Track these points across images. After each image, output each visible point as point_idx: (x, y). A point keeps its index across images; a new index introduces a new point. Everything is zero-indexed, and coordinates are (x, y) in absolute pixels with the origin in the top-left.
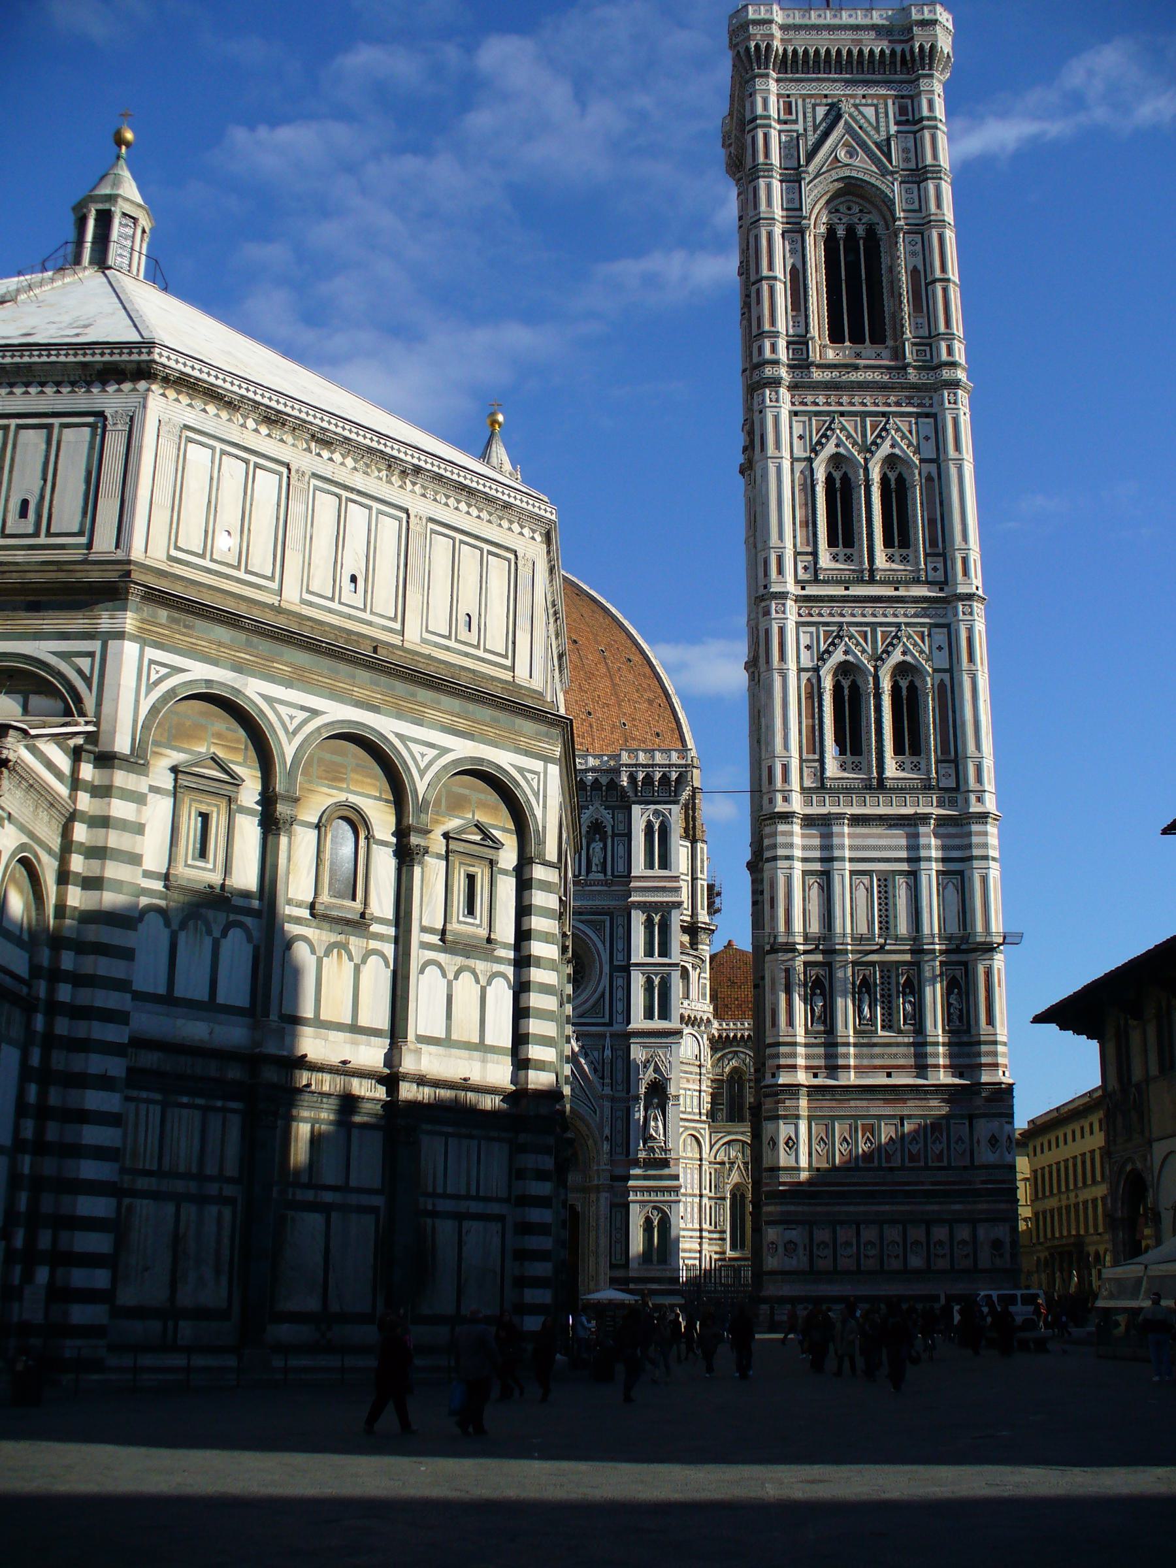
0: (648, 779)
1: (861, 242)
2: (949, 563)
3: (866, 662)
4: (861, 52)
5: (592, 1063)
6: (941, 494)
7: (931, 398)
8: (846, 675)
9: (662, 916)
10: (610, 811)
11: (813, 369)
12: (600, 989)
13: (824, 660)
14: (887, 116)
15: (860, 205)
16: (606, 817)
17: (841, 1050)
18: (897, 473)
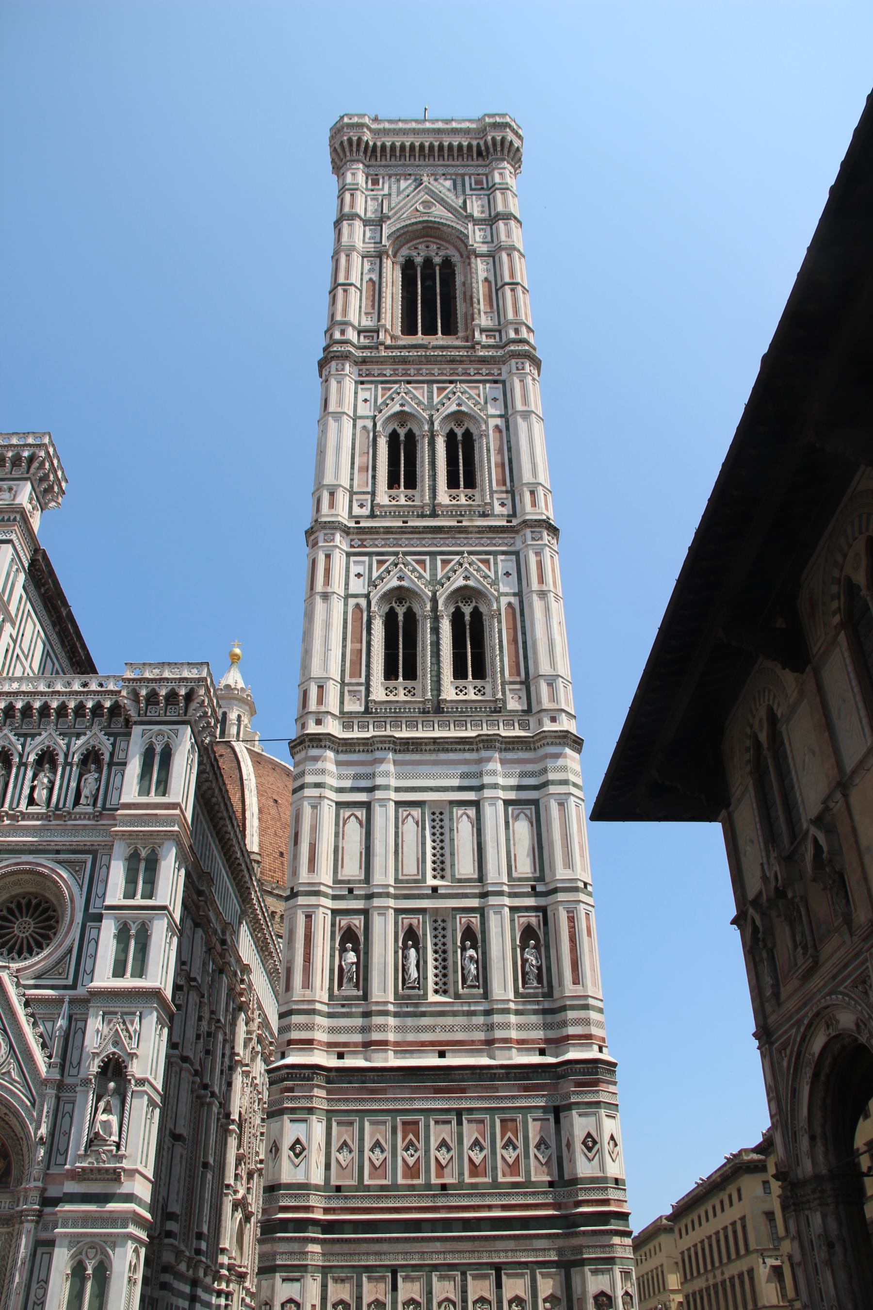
0: (152, 697)
1: (437, 268)
2: (517, 498)
3: (423, 587)
4: (441, 147)
5: (41, 1036)
6: (509, 442)
7: (500, 369)
8: (401, 603)
9: (153, 850)
10: (112, 739)
11: (382, 348)
12: (68, 942)
13: (376, 586)
14: (464, 185)
15: (437, 244)
16: (105, 745)
17: (377, 1020)
18: (464, 428)
